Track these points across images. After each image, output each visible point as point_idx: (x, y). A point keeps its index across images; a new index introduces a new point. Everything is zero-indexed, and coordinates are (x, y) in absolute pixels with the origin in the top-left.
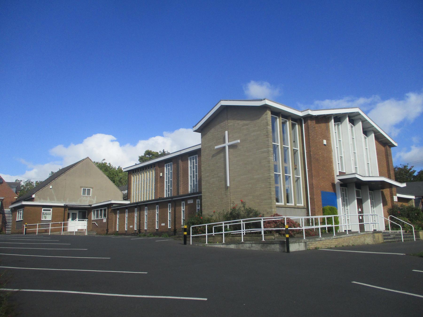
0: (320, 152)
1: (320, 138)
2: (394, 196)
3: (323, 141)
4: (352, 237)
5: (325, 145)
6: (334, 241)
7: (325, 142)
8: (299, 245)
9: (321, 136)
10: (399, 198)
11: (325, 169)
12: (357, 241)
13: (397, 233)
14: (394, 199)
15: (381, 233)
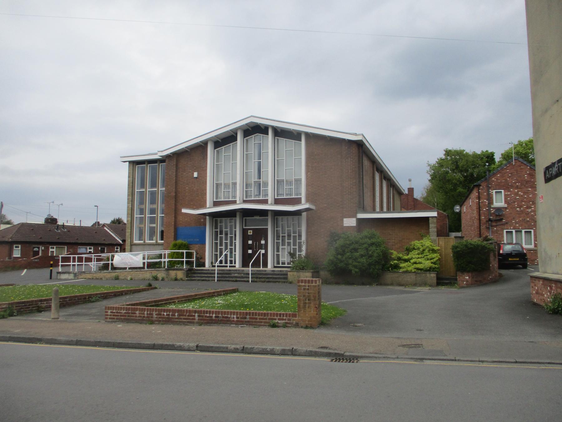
0: (187, 187)
1: (190, 172)
2: (345, 220)
3: (193, 174)
4: (132, 272)
5: (196, 178)
6: (106, 275)
7: (196, 175)
8: (69, 276)
9: (190, 170)
10: (360, 221)
11: (192, 203)
12: (139, 276)
13: (254, 271)
14: (345, 222)
15: (183, 271)
